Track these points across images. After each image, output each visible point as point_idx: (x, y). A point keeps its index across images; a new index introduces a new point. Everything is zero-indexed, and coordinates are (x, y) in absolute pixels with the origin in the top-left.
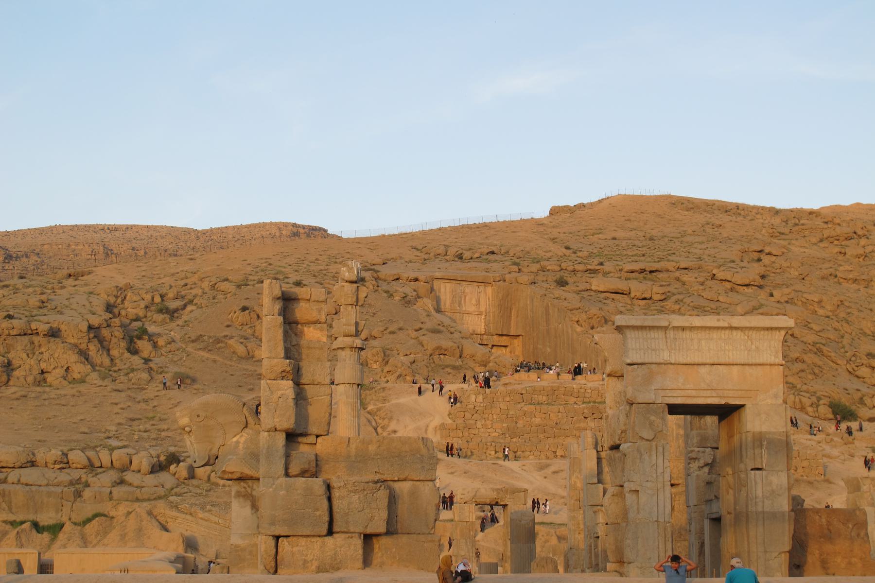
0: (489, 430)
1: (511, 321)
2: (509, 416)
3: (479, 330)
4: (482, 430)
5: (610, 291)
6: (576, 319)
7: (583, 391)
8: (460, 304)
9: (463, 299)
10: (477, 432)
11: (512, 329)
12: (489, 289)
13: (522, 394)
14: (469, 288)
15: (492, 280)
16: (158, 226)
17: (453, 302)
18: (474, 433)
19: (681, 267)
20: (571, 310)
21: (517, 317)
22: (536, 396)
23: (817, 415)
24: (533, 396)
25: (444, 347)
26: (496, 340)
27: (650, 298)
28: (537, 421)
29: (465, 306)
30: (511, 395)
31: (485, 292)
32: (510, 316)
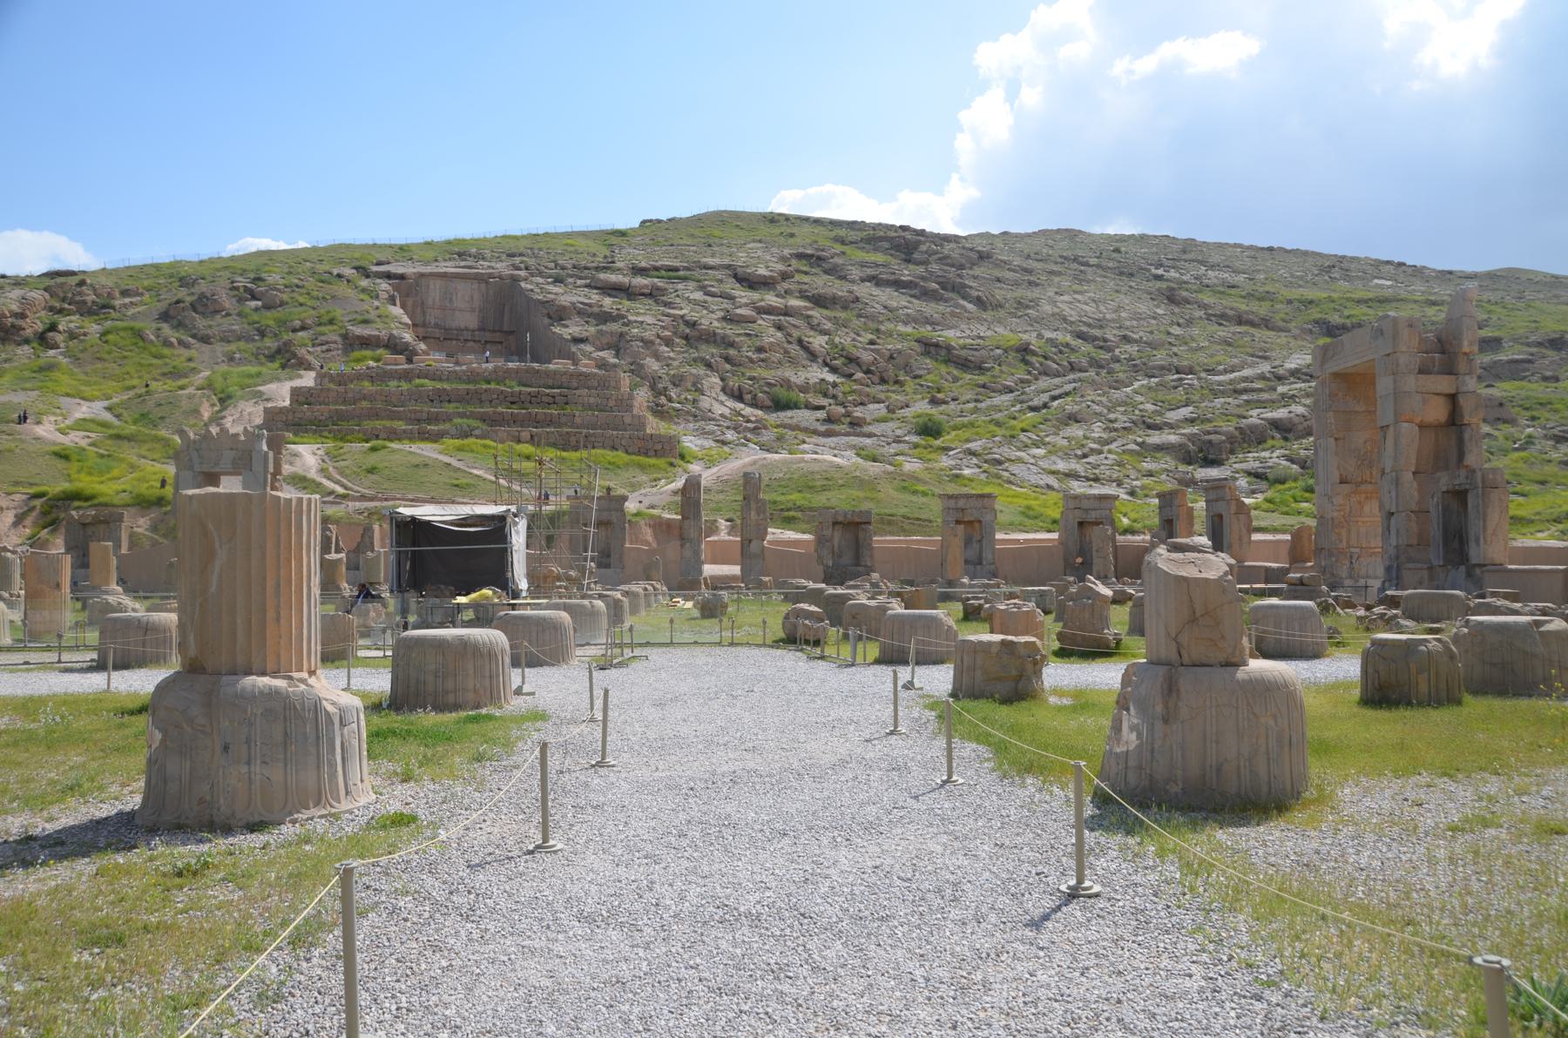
27: (650, 294)
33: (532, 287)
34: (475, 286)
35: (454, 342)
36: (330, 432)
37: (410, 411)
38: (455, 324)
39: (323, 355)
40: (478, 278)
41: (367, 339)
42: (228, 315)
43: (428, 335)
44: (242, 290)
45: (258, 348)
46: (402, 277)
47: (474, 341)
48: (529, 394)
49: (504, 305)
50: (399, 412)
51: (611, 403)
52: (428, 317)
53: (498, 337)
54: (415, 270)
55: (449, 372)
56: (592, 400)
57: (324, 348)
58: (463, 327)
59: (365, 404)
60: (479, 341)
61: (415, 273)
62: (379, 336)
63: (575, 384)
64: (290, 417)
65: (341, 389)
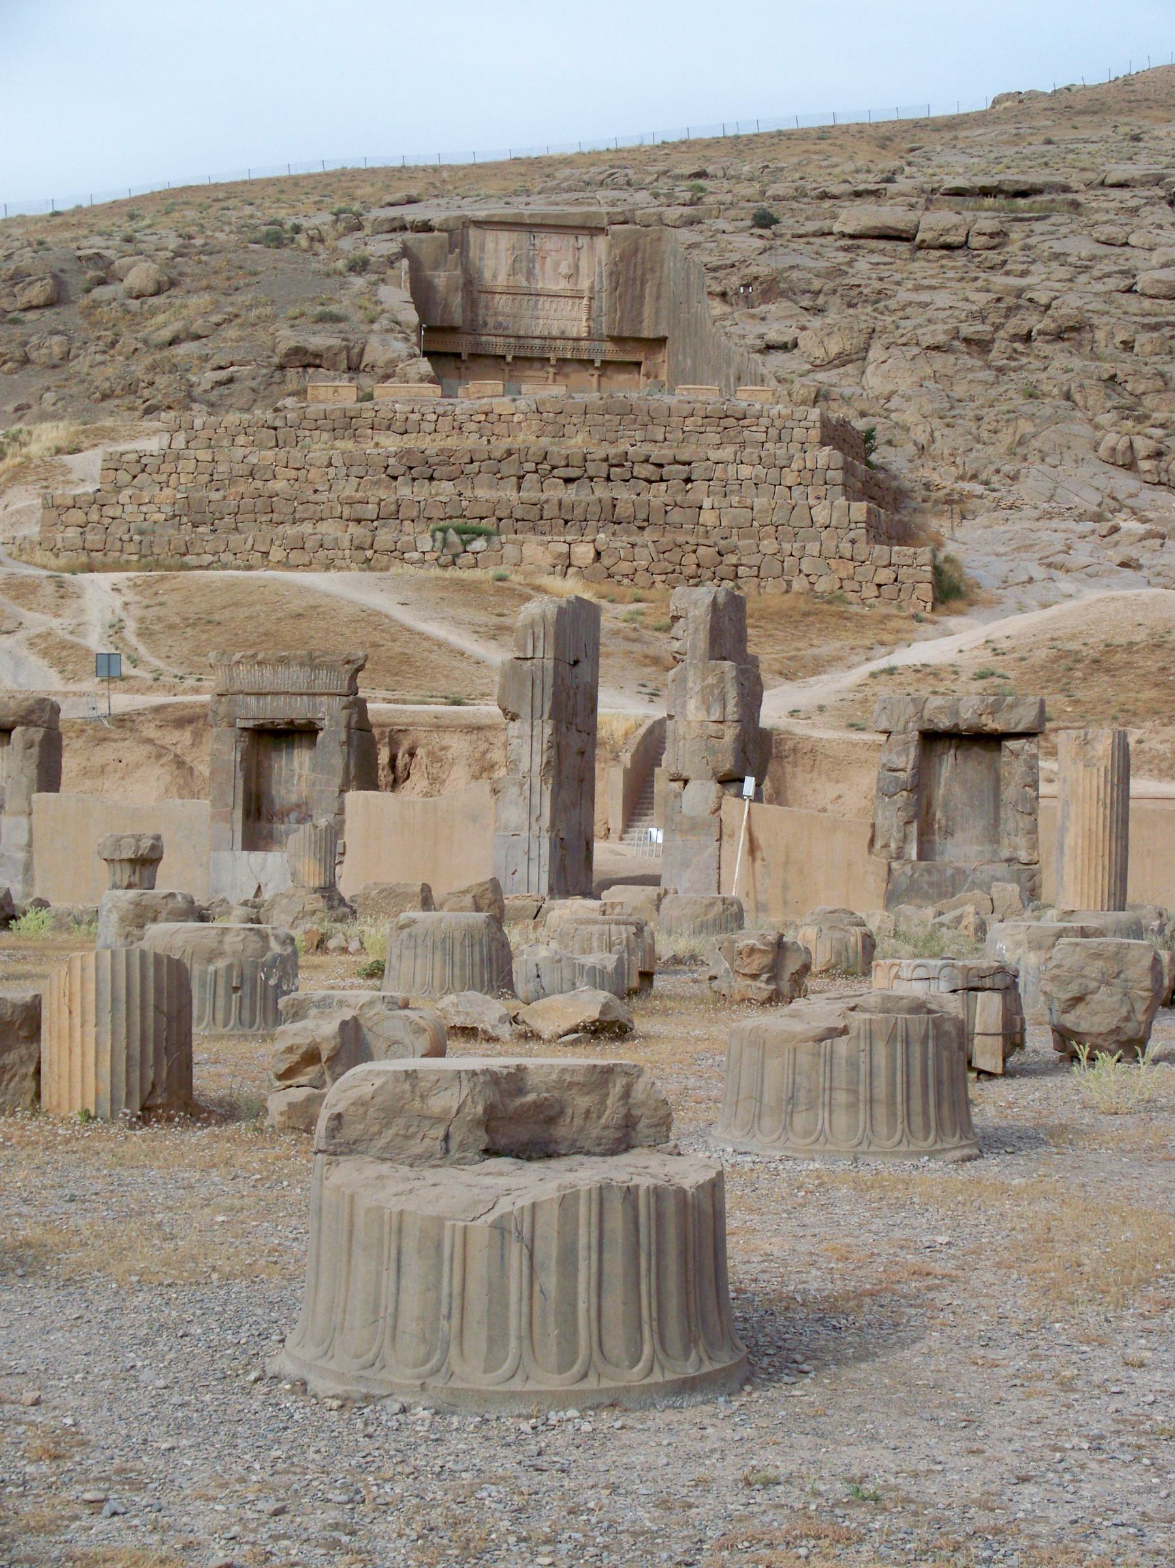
0: (144, 509)
1: (642, 305)
2: (215, 477)
3: (575, 330)
4: (129, 508)
5: (871, 233)
6: (719, 289)
7: (415, 417)
8: (530, 274)
9: (537, 266)
10: (117, 512)
11: (645, 323)
12: (601, 242)
13: (275, 429)
14: (550, 243)
15: (606, 221)
16: (236, 184)
17: (513, 272)
18: (111, 514)
19: (1109, 181)
20: (715, 270)
21: (658, 298)
22: (307, 433)
23: (1164, 478)
24: (299, 433)
25: (311, 348)
26: (610, 351)
27: (964, 245)
28: (279, 485)
29: (544, 278)
30: (249, 430)
31: (592, 248)
32: (642, 297)
33: (700, 239)
41: (317, 355)
46: (426, 227)
51: (790, 478)
52: (482, 312)
54: (458, 213)
58: (555, 332)
60: (592, 362)
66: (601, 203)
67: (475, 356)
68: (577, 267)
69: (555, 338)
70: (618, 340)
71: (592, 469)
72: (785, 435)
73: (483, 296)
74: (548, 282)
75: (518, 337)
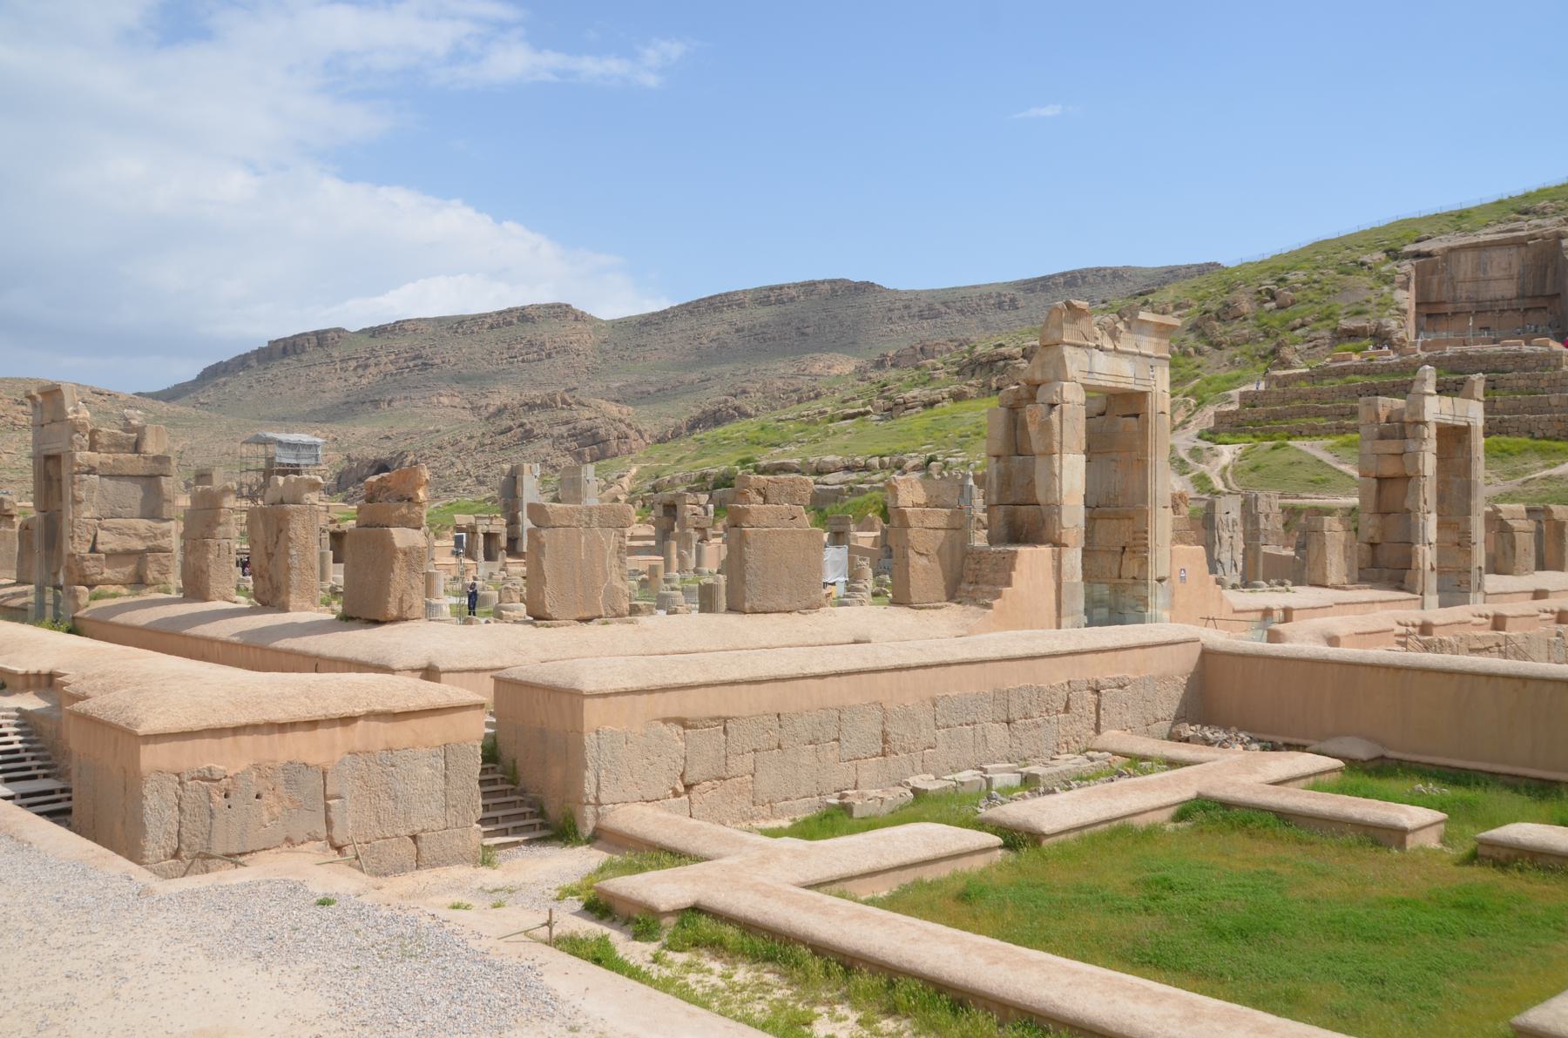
8: (1485, 271)
12: (1523, 250)
26: (1528, 303)
34: (1514, 251)
35: (1489, 314)
36: (1262, 431)
37: (1335, 408)
38: (1490, 295)
39: (1311, 352)
40: (1519, 243)
41: (1354, 331)
42: (1245, 319)
43: (1458, 310)
44: (1264, 293)
45: (1257, 350)
46: (1429, 255)
47: (1513, 310)
48: (1455, 381)
49: (1546, 267)
50: (1325, 409)
51: (1543, 384)
53: (1540, 303)
55: (1383, 365)
56: (1521, 382)
57: (1311, 344)
58: (1499, 297)
59: (1298, 403)
60: (1519, 309)
61: (1443, 249)
62: (1365, 327)
63: (1511, 367)
64: (1235, 419)
65: (1281, 390)
66: (1527, 227)
67: (1454, 314)
68: (1510, 264)
69: (1497, 301)
70: (1534, 297)
71: (1448, 386)
72: (1546, 364)
73: (1460, 284)
74: (1495, 272)
75: (1477, 302)
